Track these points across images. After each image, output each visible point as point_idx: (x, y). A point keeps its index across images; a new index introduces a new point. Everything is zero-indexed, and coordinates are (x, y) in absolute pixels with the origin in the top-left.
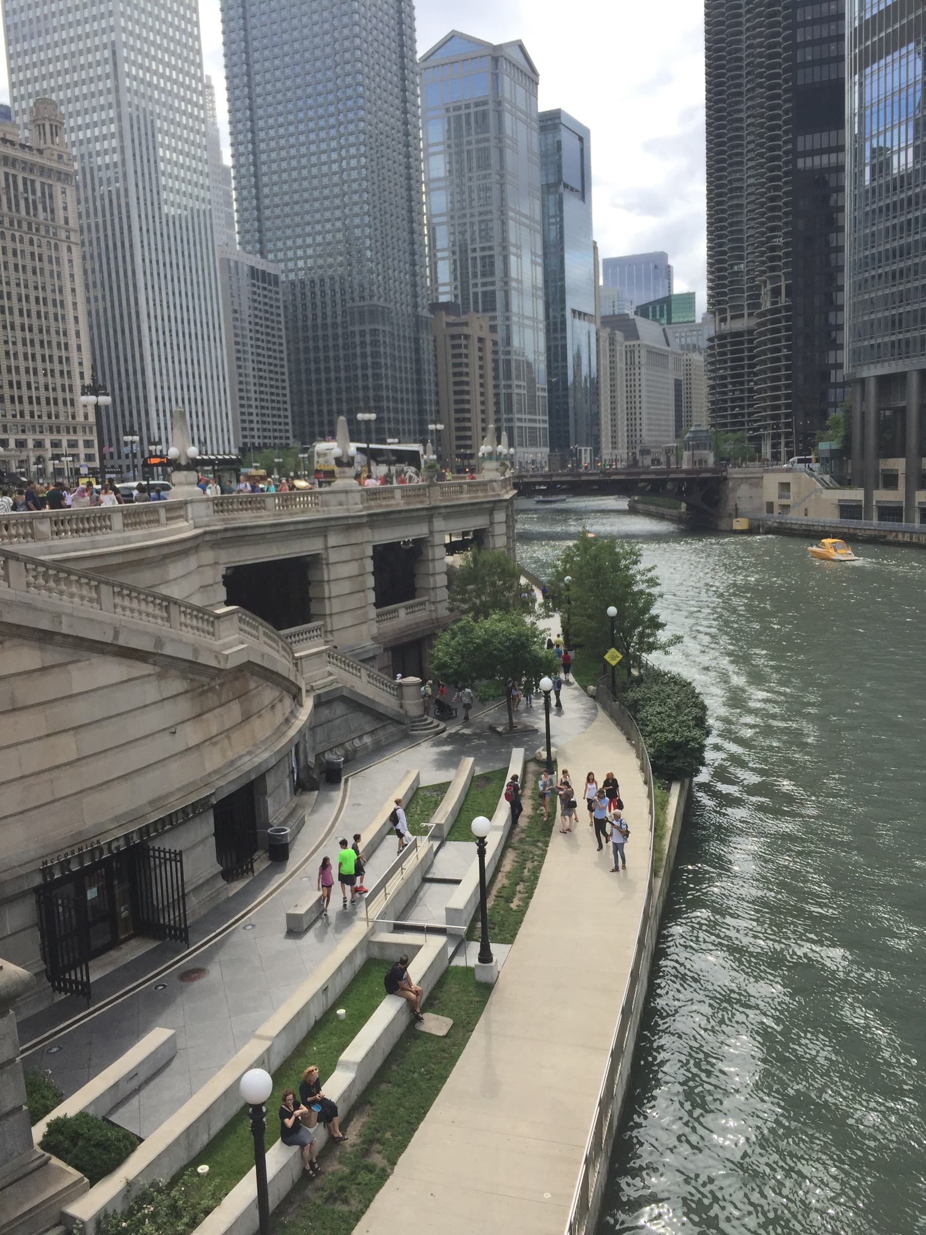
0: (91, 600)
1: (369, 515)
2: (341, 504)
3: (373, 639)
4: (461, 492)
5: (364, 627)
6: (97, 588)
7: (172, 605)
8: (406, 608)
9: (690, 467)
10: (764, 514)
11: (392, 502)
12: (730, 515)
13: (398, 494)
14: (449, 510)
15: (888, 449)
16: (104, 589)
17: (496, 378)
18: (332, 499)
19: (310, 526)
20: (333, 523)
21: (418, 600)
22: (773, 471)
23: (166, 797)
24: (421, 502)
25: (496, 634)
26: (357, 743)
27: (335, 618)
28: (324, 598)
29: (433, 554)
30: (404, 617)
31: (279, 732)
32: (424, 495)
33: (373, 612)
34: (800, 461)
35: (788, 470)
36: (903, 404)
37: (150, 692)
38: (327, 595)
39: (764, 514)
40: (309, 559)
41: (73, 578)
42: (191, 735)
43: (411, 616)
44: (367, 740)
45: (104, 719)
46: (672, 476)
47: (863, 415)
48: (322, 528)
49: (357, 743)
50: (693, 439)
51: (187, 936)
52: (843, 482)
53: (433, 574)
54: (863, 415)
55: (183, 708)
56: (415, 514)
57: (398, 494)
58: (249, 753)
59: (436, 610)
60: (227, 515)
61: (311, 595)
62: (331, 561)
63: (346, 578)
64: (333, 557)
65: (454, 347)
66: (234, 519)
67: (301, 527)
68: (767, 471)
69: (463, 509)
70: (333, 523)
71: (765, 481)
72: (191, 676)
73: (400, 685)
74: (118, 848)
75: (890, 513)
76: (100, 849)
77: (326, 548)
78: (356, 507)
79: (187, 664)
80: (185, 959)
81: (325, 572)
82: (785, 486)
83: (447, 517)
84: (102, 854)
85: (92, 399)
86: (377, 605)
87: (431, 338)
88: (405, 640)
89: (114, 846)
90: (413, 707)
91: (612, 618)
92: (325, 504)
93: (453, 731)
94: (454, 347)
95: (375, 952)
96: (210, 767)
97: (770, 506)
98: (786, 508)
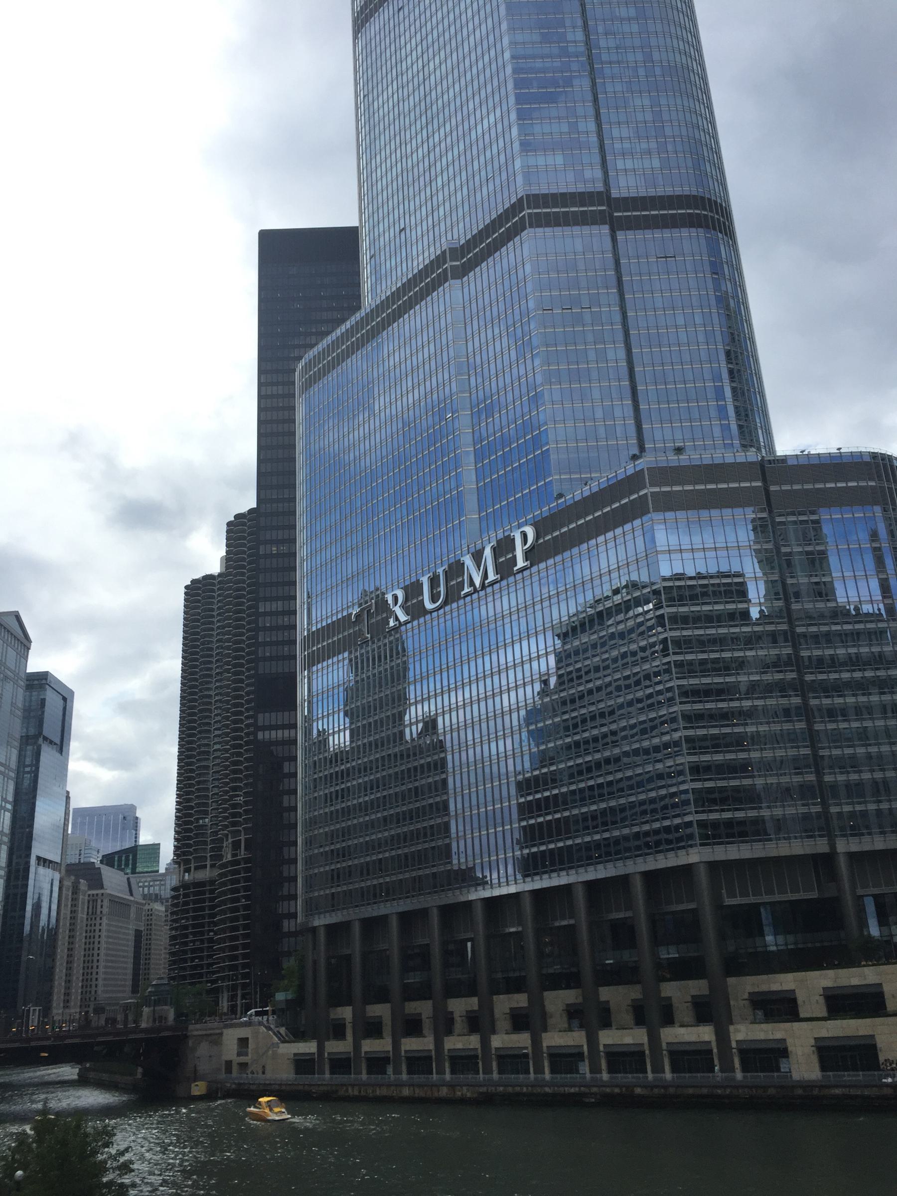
10: (222, 1076)
15: (338, 998)
34: (258, 1014)
35: (248, 1024)
39: (222, 1076)
52: (298, 1035)
68: (227, 1027)
71: (225, 1037)
82: (243, 1042)
97: (229, 1064)
98: (243, 1066)
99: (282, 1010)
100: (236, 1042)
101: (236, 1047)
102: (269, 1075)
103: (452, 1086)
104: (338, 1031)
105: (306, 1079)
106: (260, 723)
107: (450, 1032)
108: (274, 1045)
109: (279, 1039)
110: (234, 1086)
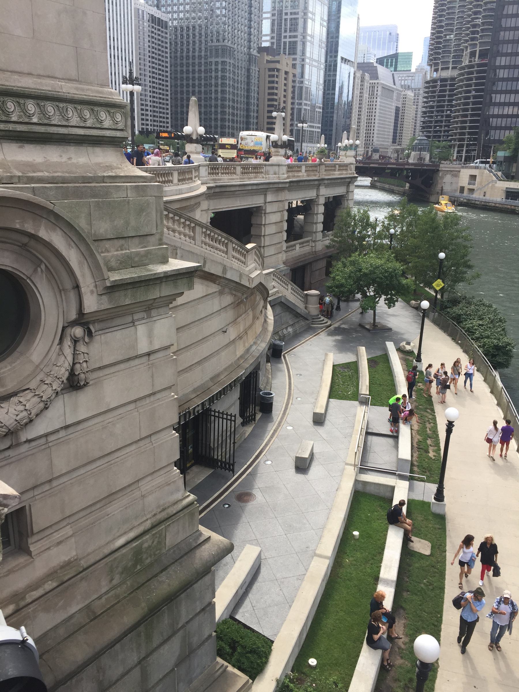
0: (190, 237)
2: (275, 174)
3: (284, 263)
4: (335, 170)
5: (280, 255)
6: (193, 229)
8: (300, 244)
9: (416, 161)
10: (458, 194)
11: (300, 174)
13: (303, 168)
14: (329, 182)
17: (293, 98)
18: (271, 169)
21: (306, 239)
22: (466, 167)
23: (218, 375)
24: (315, 175)
26: (285, 331)
31: (265, 328)
33: (285, 245)
34: (482, 162)
37: (215, 304)
38: (263, 234)
40: (255, 209)
41: (182, 220)
43: (302, 249)
44: (290, 330)
45: (192, 323)
46: (406, 167)
49: (285, 331)
50: (419, 144)
53: (316, 223)
55: (230, 315)
57: (303, 168)
59: (315, 246)
60: (215, 177)
63: (273, 222)
65: (270, 76)
67: (255, 187)
69: (336, 181)
71: (461, 174)
72: (234, 292)
73: (307, 295)
76: (189, 412)
78: (284, 176)
79: (234, 285)
80: (235, 483)
81: (263, 218)
83: (327, 186)
84: (190, 417)
85: (130, 87)
86: (286, 241)
87: (257, 69)
88: (300, 264)
89: (196, 410)
90: (314, 309)
91: (441, 260)
92: (267, 173)
93: (336, 325)
94: (270, 76)
95: (360, 487)
96: (239, 353)
100: (468, 176)
101: (468, 179)
102: (488, 198)
109: (497, 178)
110: (465, 201)
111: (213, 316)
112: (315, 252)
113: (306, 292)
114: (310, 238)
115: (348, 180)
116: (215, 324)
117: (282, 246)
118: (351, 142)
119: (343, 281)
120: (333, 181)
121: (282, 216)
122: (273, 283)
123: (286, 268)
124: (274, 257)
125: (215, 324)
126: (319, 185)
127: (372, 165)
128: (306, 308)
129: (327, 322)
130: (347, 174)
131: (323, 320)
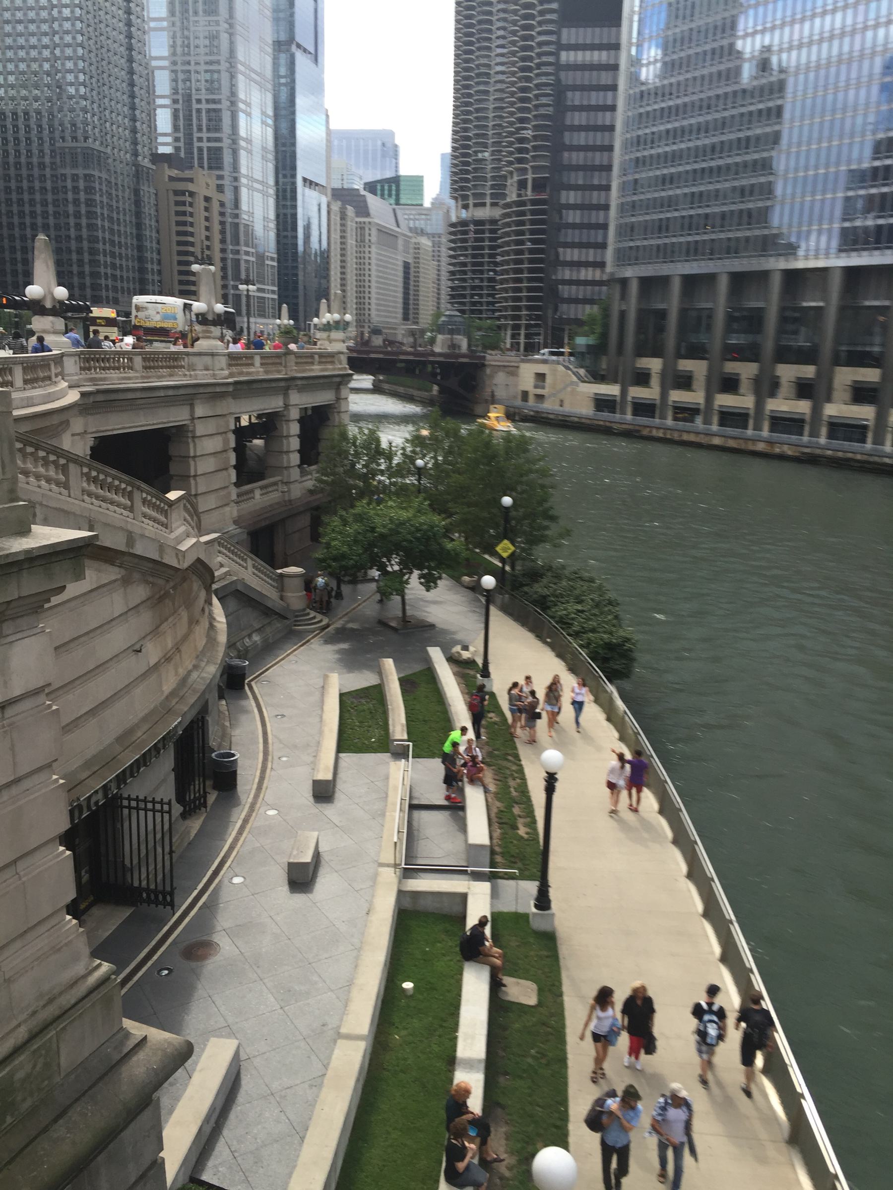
1: (236, 383)
3: (235, 522)
4: (312, 363)
5: (227, 509)
7: (135, 490)
8: (262, 488)
9: (446, 350)
11: (252, 370)
12: (486, 401)
13: (257, 360)
14: (304, 382)
16: (72, 467)
19: (182, 392)
20: (201, 390)
23: (130, 732)
24: (279, 372)
25: (402, 524)
26: (247, 641)
27: (200, 499)
28: (189, 476)
29: (288, 428)
30: (261, 498)
32: (281, 364)
33: (234, 492)
35: (545, 362)
36: (661, 306)
37: (116, 603)
38: (192, 473)
42: (153, 653)
43: (266, 498)
44: (256, 638)
46: (431, 359)
47: (623, 315)
48: (188, 396)
49: (247, 641)
51: (172, 900)
53: (288, 452)
54: (623, 315)
55: (146, 618)
56: (274, 385)
58: (196, 667)
61: (172, 472)
62: (198, 434)
64: (200, 429)
66: (104, 379)
69: (316, 381)
70: (201, 390)
72: (151, 579)
73: (281, 575)
74: (97, 803)
75: (643, 409)
77: (193, 419)
79: (151, 565)
83: (301, 390)
86: (237, 484)
88: (263, 524)
90: (296, 598)
99: (582, 354)
103: (770, 443)
104: (642, 378)
105: (606, 415)
106: (564, 41)
107: (773, 394)
108: (572, 383)
111: (114, 623)
112: (290, 501)
113: (279, 571)
114: (279, 478)
115: (338, 379)
116: (119, 638)
117: (229, 493)
118: (337, 316)
119: (345, 549)
120: (311, 382)
121: (226, 441)
122: (220, 559)
123: (239, 530)
124: (216, 513)
125: (119, 638)
126: (288, 388)
127: (373, 356)
128: (282, 598)
129: (321, 621)
130: (334, 369)
131: (314, 618)
